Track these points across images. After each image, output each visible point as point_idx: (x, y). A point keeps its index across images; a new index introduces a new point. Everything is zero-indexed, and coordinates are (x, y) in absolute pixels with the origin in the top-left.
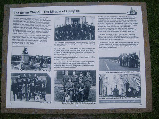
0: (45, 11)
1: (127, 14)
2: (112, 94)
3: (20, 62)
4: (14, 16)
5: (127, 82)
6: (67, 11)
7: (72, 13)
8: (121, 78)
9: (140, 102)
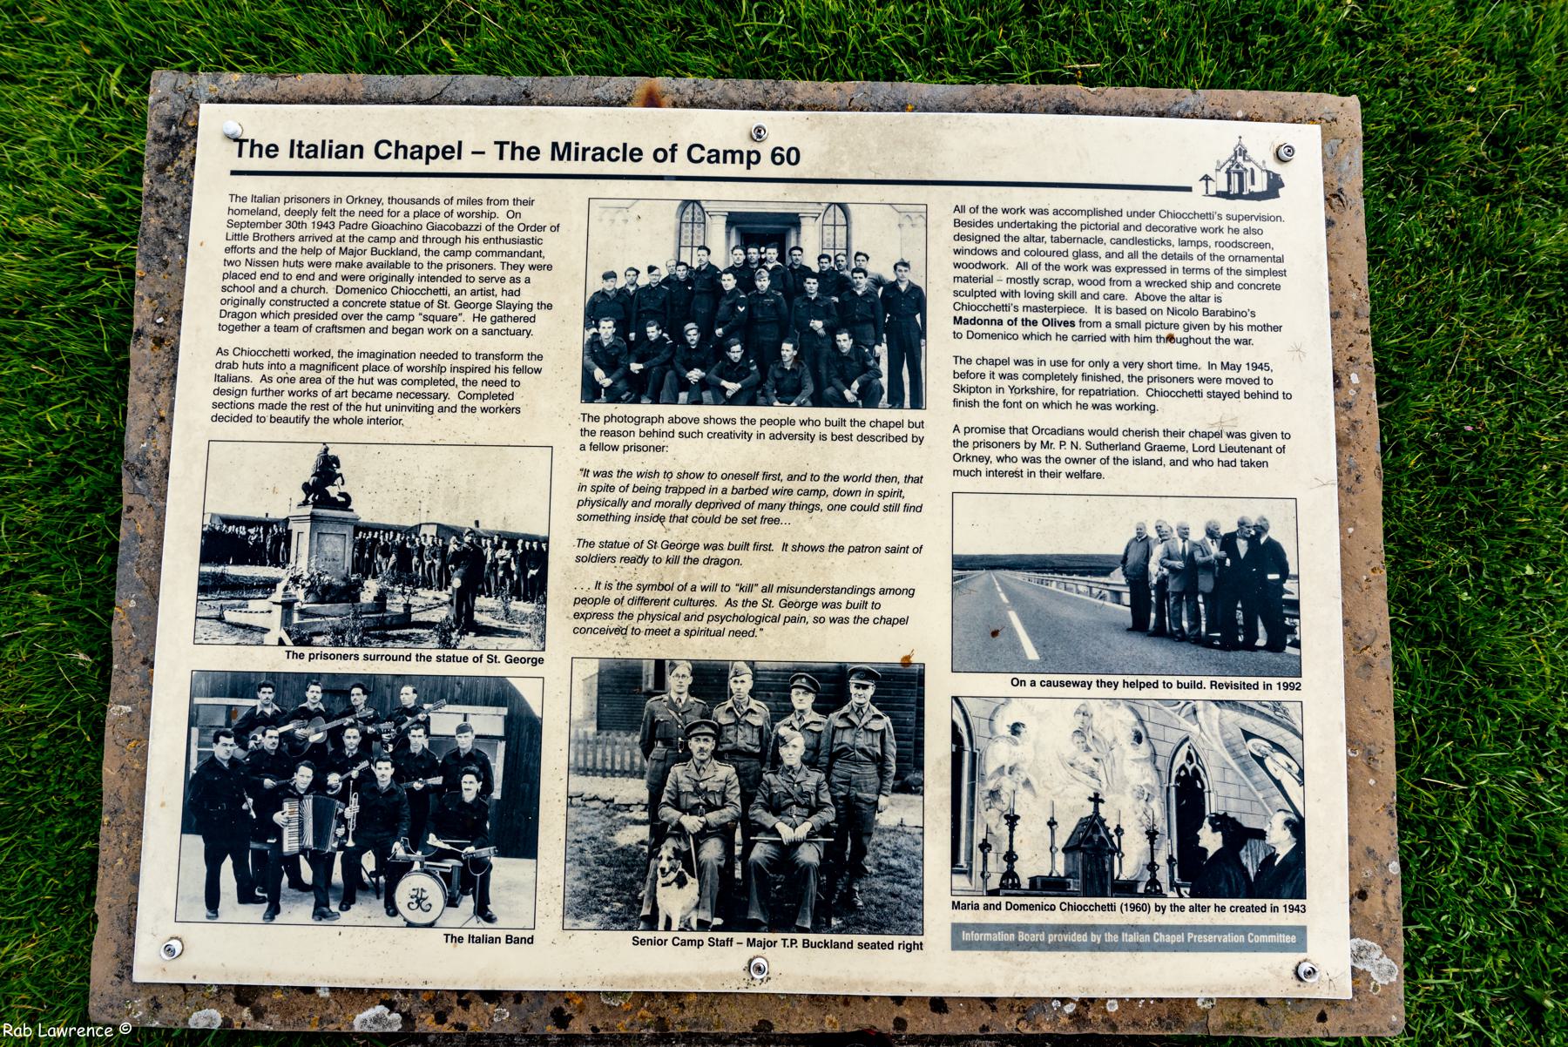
0: (502, 144)
1: (1199, 187)
2: (1060, 870)
3: (279, 580)
4: (234, 173)
5: (1190, 768)
6: (696, 153)
7: (738, 170)
9: (1301, 946)
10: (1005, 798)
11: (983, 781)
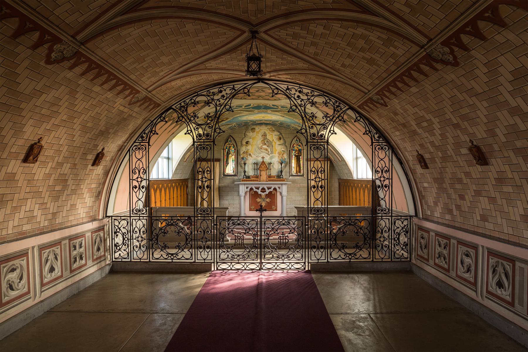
8: (280, 139)
10: (245, 159)
11: (240, 155)
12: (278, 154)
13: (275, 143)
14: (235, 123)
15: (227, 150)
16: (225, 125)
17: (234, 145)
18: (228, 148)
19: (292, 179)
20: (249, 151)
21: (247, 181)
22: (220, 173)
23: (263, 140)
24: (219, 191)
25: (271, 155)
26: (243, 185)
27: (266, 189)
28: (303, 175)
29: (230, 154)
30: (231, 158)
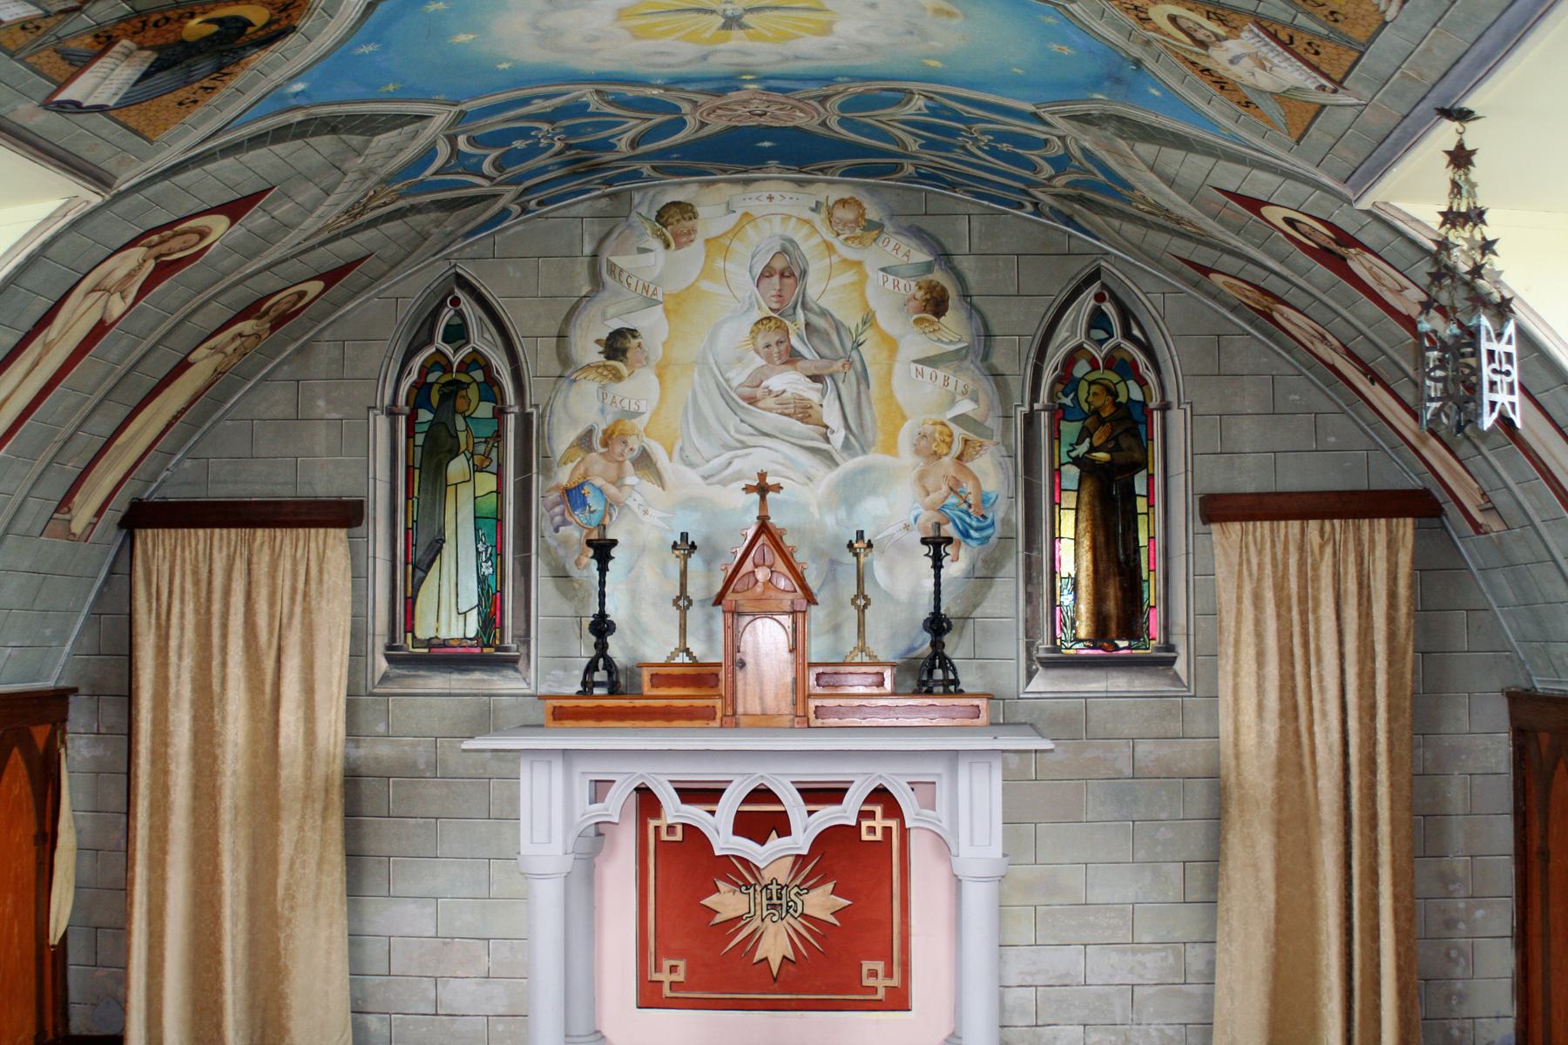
5: (1099, 356)
8: (936, 304)
10: (594, 502)
11: (547, 470)
12: (918, 452)
13: (891, 344)
14: (441, 118)
15: (425, 416)
16: (329, 126)
17: (487, 368)
18: (435, 398)
19: (1058, 696)
20: (640, 423)
21: (600, 715)
22: (358, 635)
23: (772, 322)
24: (353, 812)
25: (848, 464)
26: (558, 769)
27: (792, 804)
28: (1162, 662)
29: (454, 453)
30: (465, 493)
